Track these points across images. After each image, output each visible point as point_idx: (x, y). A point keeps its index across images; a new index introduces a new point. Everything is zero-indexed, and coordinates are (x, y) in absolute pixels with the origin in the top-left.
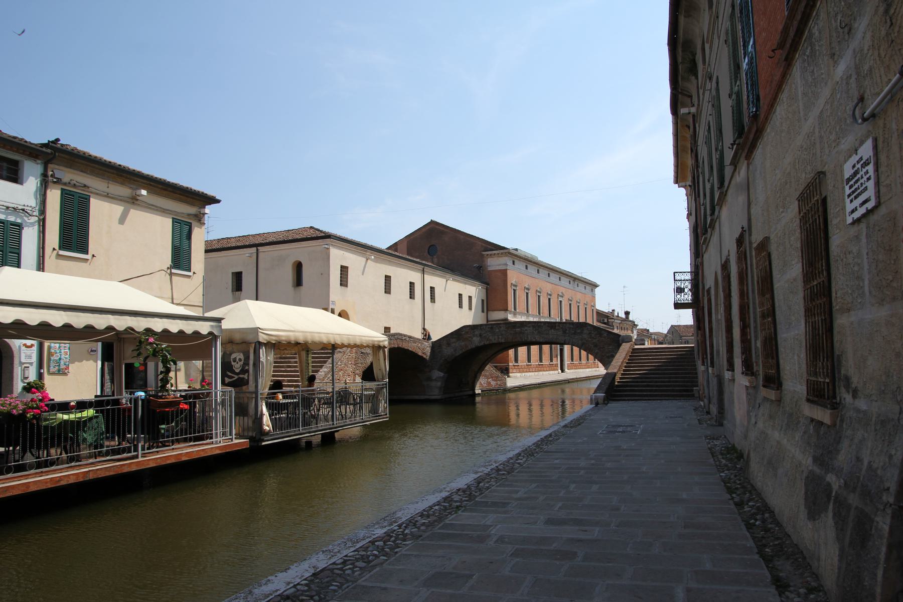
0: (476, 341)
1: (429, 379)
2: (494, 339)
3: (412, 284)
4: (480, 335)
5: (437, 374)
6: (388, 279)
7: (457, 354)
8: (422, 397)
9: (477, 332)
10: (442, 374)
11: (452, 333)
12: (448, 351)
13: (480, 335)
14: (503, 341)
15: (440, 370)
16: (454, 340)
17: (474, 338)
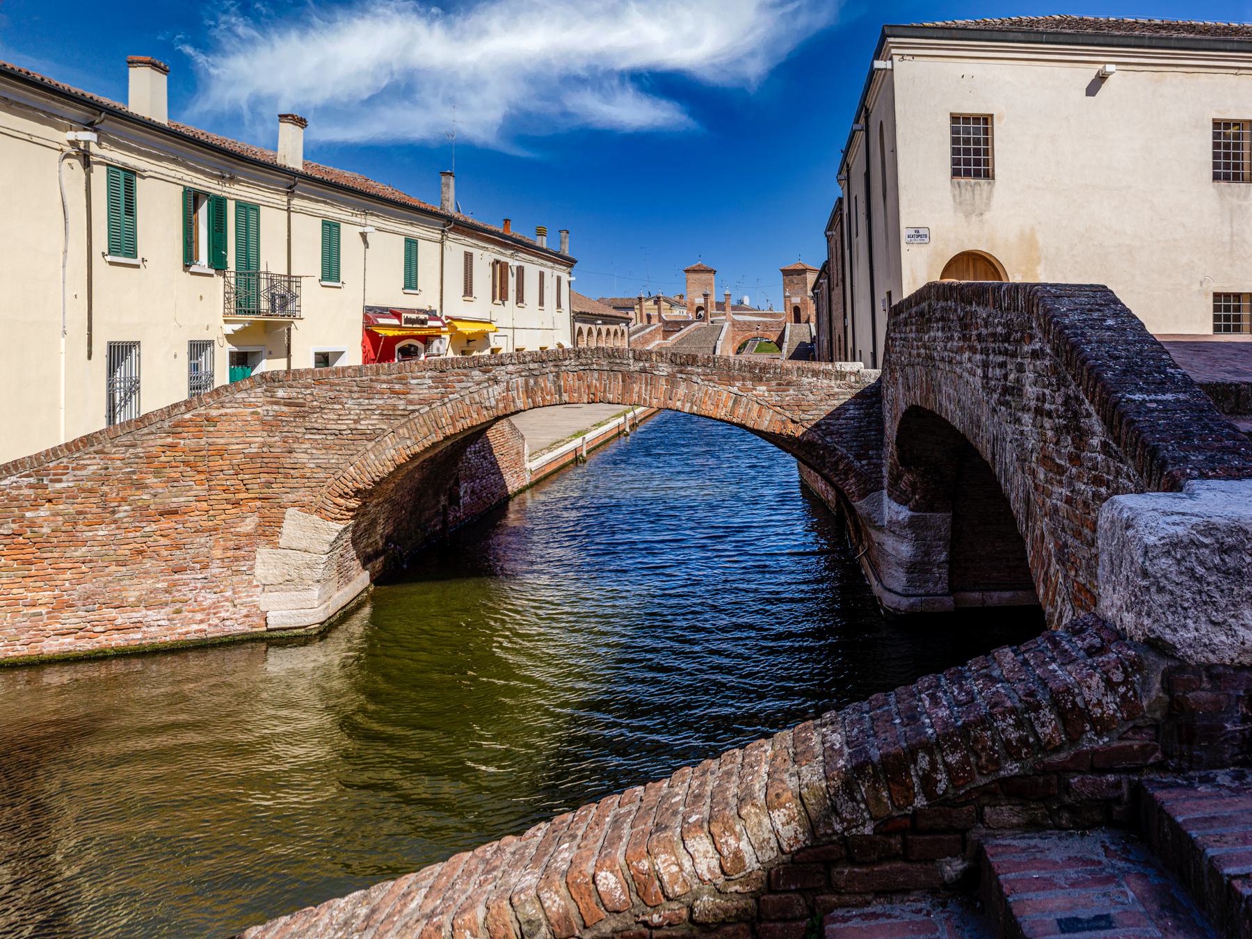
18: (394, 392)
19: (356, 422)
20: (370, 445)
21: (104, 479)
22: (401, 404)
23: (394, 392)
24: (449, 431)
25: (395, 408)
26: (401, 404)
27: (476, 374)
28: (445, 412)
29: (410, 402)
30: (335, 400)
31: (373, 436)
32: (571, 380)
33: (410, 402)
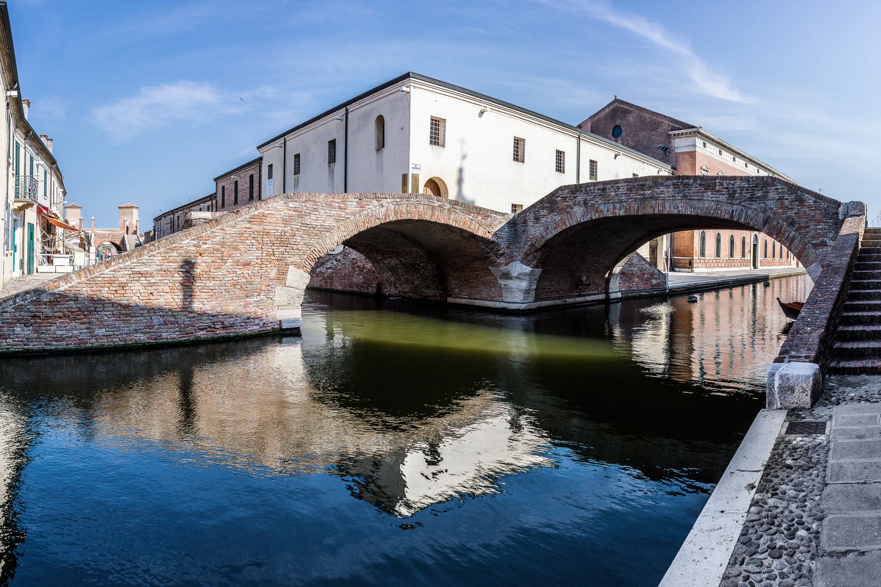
0: (579, 215)
1: (507, 276)
2: (607, 211)
3: (560, 155)
4: (585, 203)
5: (519, 268)
6: (518, 143)
7: (549, 237)
8: (498, 305)
9: (580, 198)
10: (528, 269)
11: (542, 201)
12: (536, 232)
13: (585, 203)
14: (622, 214)
15: (525, 261)
16: (544, 212)
17: (576, 209)
18: (340, 208)
19: (324, 222)
20: (328, 234)
21: (223, 244)
22: (343, 214)
23: (340, 208)
24: (362, 229)
25: (340, 216)
26: (343, 214)
27: (374, 201)
28: (360, 219)
29: (347, 214)
30: (315, 210)
31: (329, 229)
32: (413, 209)
33: (347, 214)
